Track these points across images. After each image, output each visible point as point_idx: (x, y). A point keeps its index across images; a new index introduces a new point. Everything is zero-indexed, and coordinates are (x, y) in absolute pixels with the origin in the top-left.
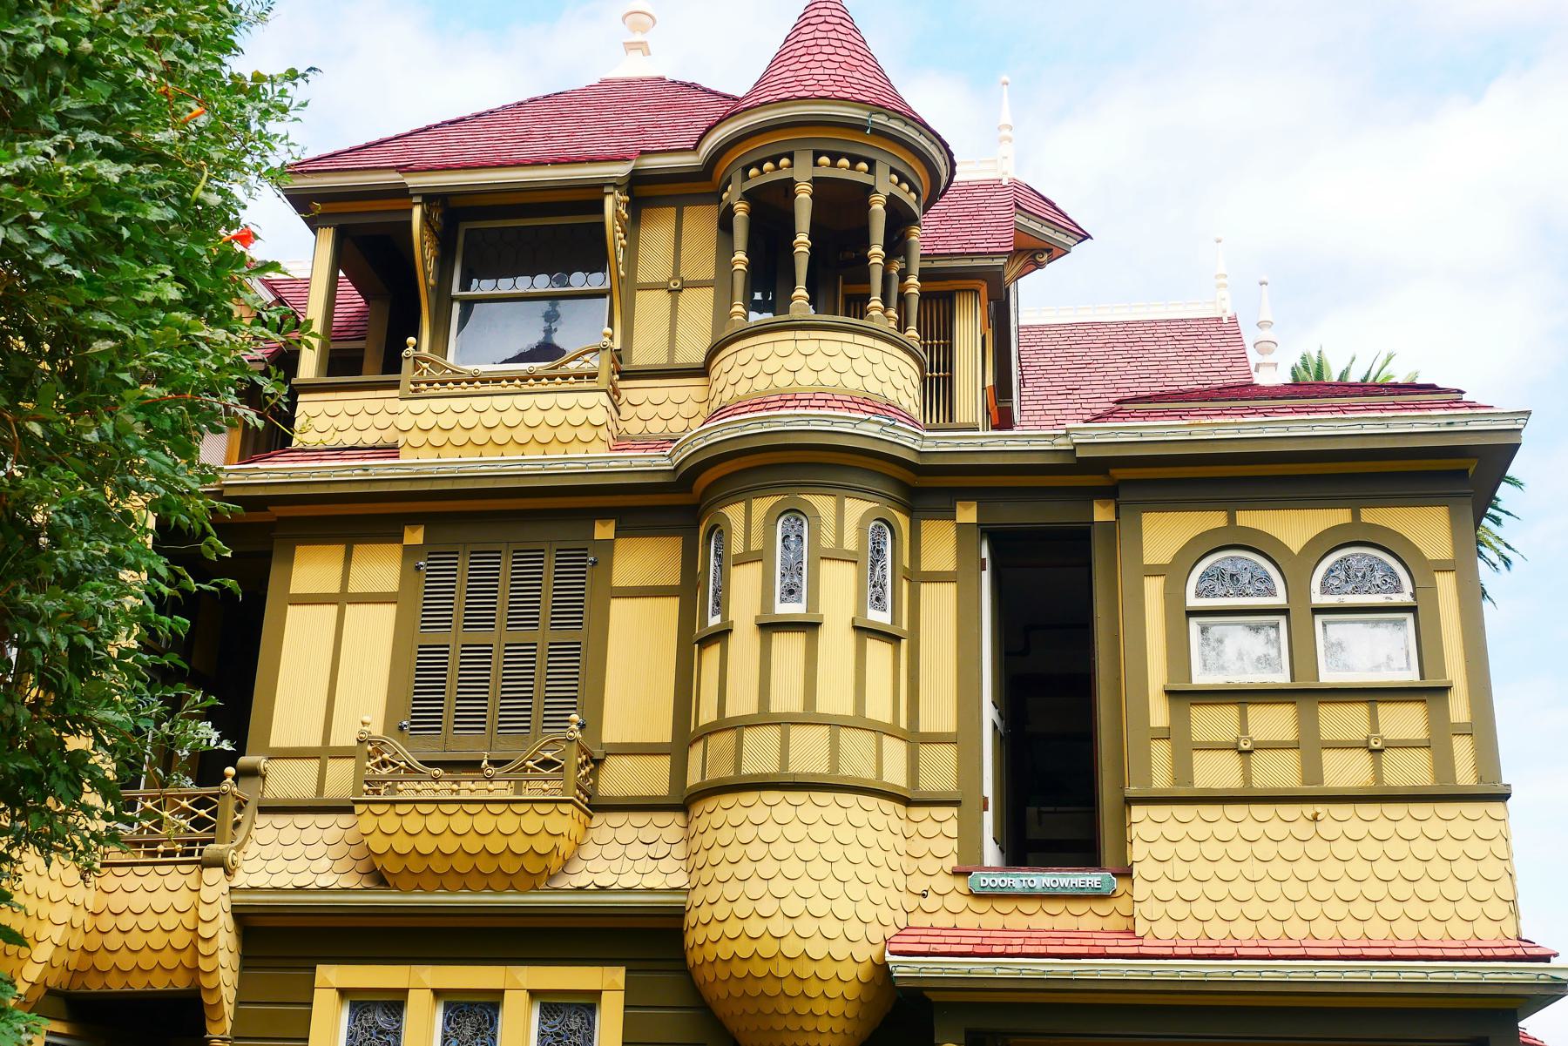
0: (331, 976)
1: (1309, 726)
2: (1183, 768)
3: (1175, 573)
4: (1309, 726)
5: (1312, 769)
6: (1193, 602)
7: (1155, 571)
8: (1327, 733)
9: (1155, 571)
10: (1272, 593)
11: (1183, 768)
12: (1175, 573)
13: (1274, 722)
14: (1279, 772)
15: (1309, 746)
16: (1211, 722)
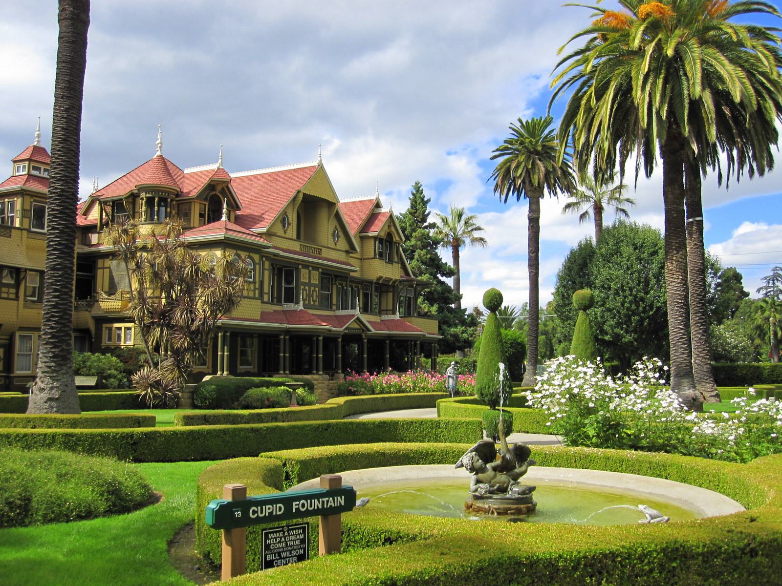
0: (105, 325)
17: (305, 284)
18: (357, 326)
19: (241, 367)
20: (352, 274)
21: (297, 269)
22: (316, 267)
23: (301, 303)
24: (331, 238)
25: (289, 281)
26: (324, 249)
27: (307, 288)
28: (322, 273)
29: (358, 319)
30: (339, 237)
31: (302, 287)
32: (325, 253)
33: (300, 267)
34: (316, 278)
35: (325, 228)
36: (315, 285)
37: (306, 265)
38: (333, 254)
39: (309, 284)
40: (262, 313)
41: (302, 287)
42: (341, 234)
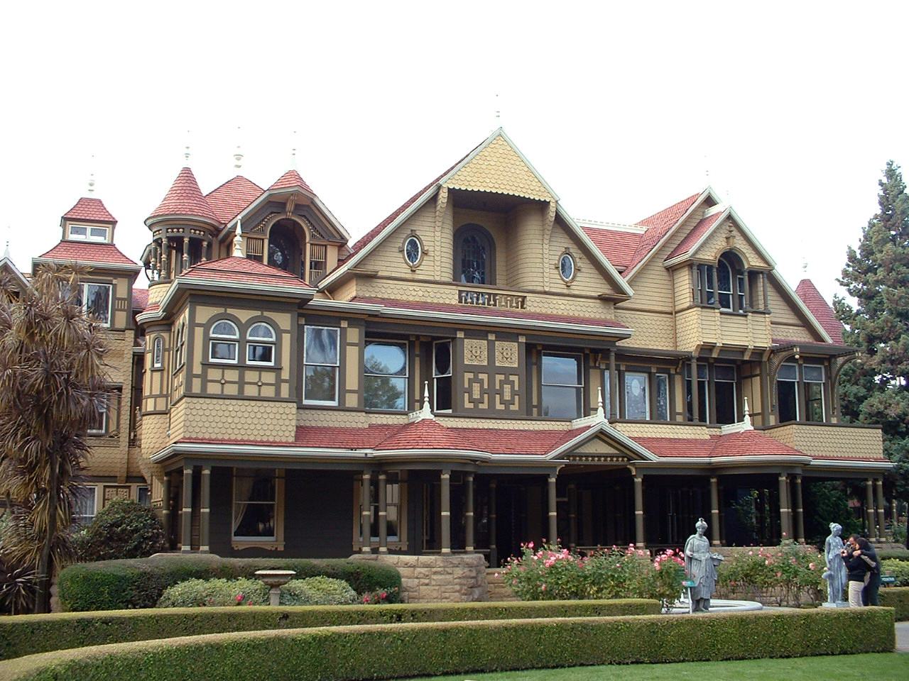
1: (242, 377)
2: (204, 387)
3: (206, 327)
4: (242, 377)
5: (241, 390)
6: (212, 335)
7: (199, 325)
8: (247, 380)
9: (199, 325)
10: (235, 335)
11: (204, 387)
12: (206, 327)
13: (232, 375)
14: (232, 390)
15: (241, 383)
16: (214, 374)
17: (476, 370)
22: (506, 333)
24: (555, 274)
25: (443, 367)
26: (530, 297)
31: (468, 376)
32: (534, 304)
33: (460, 335)
34: (509, 354)
35: (538, 257)
36: (507, 372)
37: (477, 331)
39: (491, 369)
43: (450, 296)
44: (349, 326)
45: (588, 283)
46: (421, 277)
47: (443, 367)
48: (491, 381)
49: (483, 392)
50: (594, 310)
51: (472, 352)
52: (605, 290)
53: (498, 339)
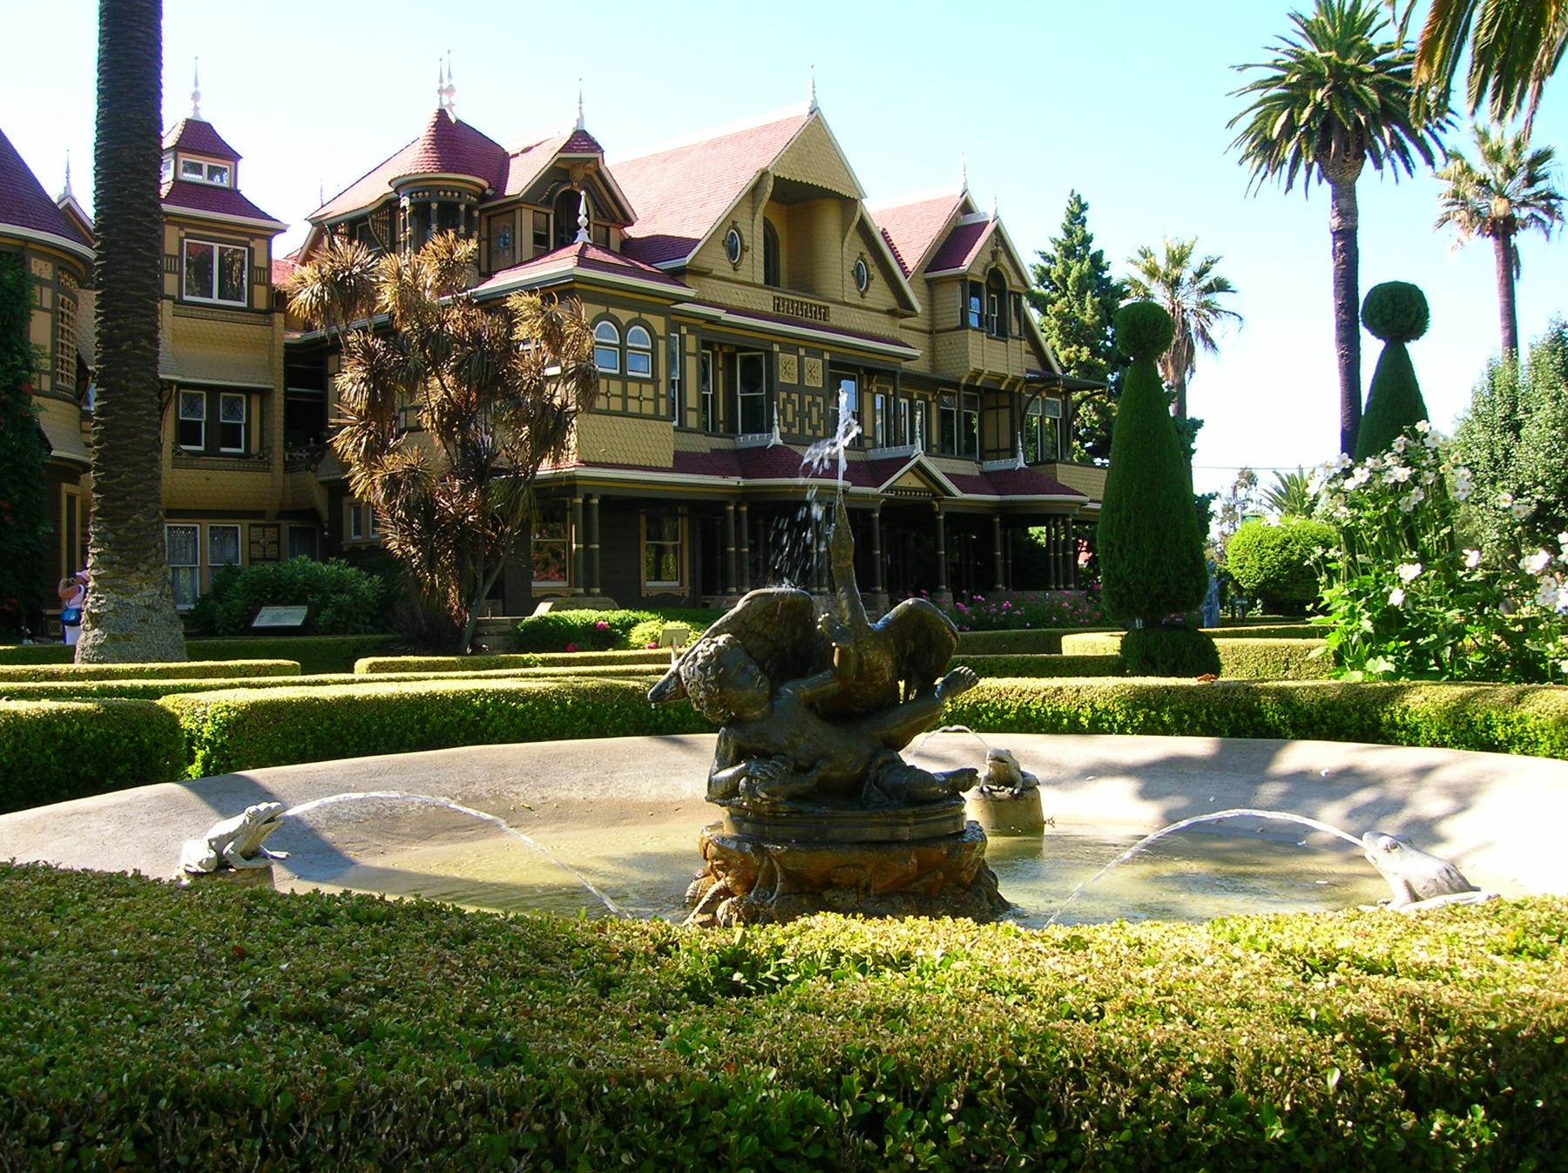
17: (789, 388)
18: (915, 483)
19: (649, 584)
20: (905, 365)
21: (770, 354)
23: (777, 431)
24: (850, 281)
27: (795, 397)
28: (832, 364)
29: (919, 465)
30: (870, 279)
31: (783, 395)
32: (837, 316)
33: (776, 348)
36: (814, 392)
37: (791, 344)
38: (859, 318)
39: (800, 388)
40: (678, 456)
41: (783, 395)
42: (875, 272)
43: (764, 300)
44: (689, 332)
45: (880, 295)
46: (741, 278)
47: (751, 382)
48: (801, 399)
49: (795, 414)
50: (883, 325)
51: (787, 369)
52: (891, 302)
53: (808, 354)
